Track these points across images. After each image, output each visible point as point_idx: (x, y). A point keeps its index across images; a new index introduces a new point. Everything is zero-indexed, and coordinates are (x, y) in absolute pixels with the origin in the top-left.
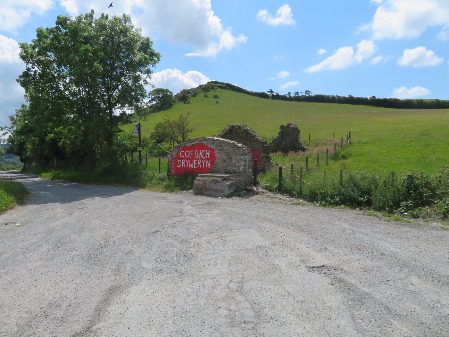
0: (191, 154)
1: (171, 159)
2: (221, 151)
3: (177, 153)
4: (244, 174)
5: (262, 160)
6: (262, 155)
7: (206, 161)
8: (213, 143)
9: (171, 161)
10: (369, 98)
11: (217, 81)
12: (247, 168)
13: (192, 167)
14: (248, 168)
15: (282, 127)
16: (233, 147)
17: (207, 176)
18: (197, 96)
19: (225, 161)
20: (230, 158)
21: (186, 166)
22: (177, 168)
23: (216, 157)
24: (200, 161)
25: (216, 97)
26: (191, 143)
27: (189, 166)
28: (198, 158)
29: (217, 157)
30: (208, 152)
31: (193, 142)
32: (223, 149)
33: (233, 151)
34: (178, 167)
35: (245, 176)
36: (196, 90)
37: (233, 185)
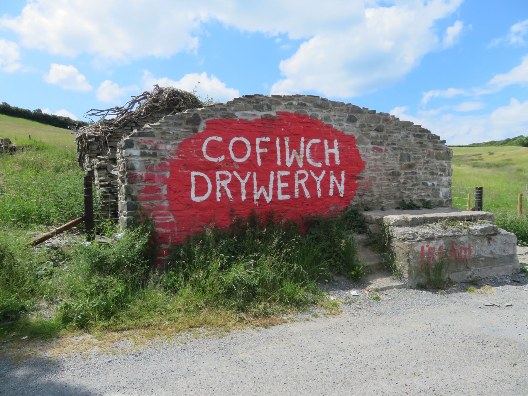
0: (259, 151)
1: (148, 168)
2: (381, 144)
8: (351, 120)
9: (149, 178)
10: (32, 111)
13: (269, 199)
16: (419, 136)
19: (395, 175)
20: (410, 166)
21: (237, 193)
24: (301, 176)
26: (260, 108)
27: (250, 194)
28: (295, 167)
31: (269, 108)
32: (386, 138)
33: (417, 147)
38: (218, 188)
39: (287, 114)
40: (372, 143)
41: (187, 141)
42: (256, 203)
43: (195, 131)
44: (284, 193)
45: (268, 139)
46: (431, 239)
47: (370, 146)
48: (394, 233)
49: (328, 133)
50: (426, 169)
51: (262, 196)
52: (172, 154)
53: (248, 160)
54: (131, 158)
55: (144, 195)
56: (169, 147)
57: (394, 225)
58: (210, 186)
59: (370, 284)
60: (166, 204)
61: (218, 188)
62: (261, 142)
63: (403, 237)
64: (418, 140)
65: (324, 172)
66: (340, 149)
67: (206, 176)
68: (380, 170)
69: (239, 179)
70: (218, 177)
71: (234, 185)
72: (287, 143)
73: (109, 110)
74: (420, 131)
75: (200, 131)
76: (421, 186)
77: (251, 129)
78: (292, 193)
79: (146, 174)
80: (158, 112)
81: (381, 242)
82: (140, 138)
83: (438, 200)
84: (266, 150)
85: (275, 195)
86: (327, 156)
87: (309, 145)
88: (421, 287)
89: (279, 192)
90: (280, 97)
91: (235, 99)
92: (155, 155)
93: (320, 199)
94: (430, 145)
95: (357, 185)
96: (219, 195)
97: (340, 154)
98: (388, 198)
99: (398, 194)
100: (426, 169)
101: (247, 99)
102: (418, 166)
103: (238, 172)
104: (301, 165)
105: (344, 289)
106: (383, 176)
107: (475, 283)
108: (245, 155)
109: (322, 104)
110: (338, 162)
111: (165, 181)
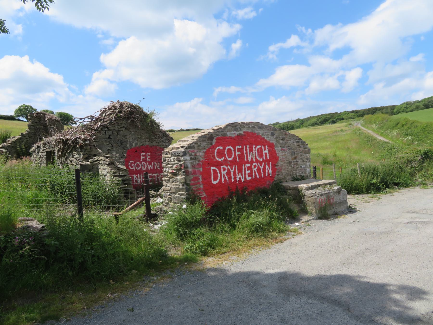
0: (237, 153)
1: (193, 166)
2: (284, 147)
3: (206, 153)
8: (273, 134)
9: (194, 173)
13: (243, 180)
19: (290, 163)
21: (230, 178)
22: (213, 186)
23: (278, 157)
26: (236, 130)
27: (235, 178)
28: (252, 162)
29: (280, 158)
30: (265, 150)
32: (286, 144)
33: (297, 147)
34: (215, 183)
38: (223, 176)
39: (247, 133)
40: (281, 147)
41: (208, 150)
42: (238, 182)
43: (211, 144)
44: (249, 176)
45: (240, 147)
46: (321, 195)
47: (280, 148)
48: (306, 193)
49: (264, 142)
50: (301, 159)
51: (240, 178)
52: (202, 158)
53: (233, 159)
54: (186, 162)
55: (193, 182)
56: (201, 153)
57: (305, 190)
58: (219, 175)
59: (302, 219)
60: (202, 186)
61: (223, 176)
62: (238, 148)
63: (311, 195)
64: (298, 144)
65: (263, 163)
66: (269, 151)
67: (217, 169)
68: (284, 161)
69: (230, 169)
70: (222, 169)
71: (229, 173)
72: (248, 149)
73: (85, 118)
75: (213, 144)
76: (300, 168)
77: (234, 141)
78: (252, 176)
79: (193, 170)
80: (121, 120)
81: (298, 198)
82: (190, 149)
83: (306, 175)
84: (240, 153)
85: (245, 178)
86: (264, 155)
87: (257, 149)
88: (320, 218)
89: (247, 175)
90: (244, 123)
91: (227, 125)
92: (195, 159)
93: (263, 178)
94: (302, 146)
95: (276, 169)
96: (223, 179)
97: (269, 153)
98: (288, 176)
99: (291, 173)
100: (301, 159)
101: (232, 125)
102: (298, 158)
103: (230, 166)
104: (254, 160)
105: (292, 223)
106: (286, 164)
107: (337, 215)
108: (232, 156)
109: (261, 126)
110: (268, 158)
111: (201, 173)
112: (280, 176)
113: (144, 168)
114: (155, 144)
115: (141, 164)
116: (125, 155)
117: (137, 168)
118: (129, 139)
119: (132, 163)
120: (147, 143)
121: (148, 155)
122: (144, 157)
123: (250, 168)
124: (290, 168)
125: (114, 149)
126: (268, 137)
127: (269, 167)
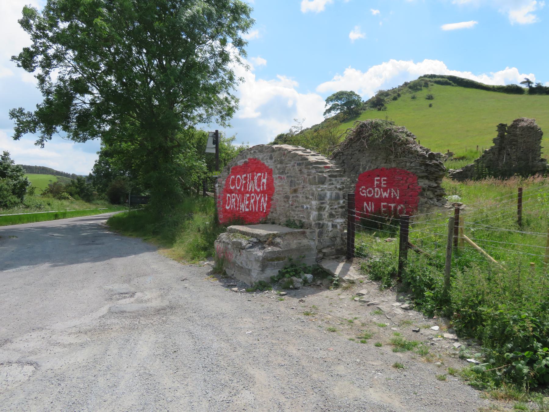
4: (317, 230)
5: (422, 195)
6: (423, 183)
7: (261, 197)
11: (433, 73)
12: (325, 214)
14: (331, 216)
15: (502, 127)
17: (237, 231)
18: (399, 99)
23: (274, 188)
25: (430, 98)
28: (251, 192)
30: (264, 178)
35: (320, 234)
36: (399, 90)
37: (278, 259)
50: (303, 193)
66: (267, 180)
74: (301, 160)
76: (301, 209)
99: (288, 214)
102: (300, 190)
112: (274, 214)
113: (377, 195)
114: (394, 165)
115: (374, 190)
116: (357, 180)
117: (368, 195)
118: (363, 162)
119: (363, 189)
120: (383, 165)
121: (384, 180)
122: (378, 183)
123: (249, 199)
124: (287, 205)
125: (346, 173)
126: (268, 162)
127: (265, 200)
